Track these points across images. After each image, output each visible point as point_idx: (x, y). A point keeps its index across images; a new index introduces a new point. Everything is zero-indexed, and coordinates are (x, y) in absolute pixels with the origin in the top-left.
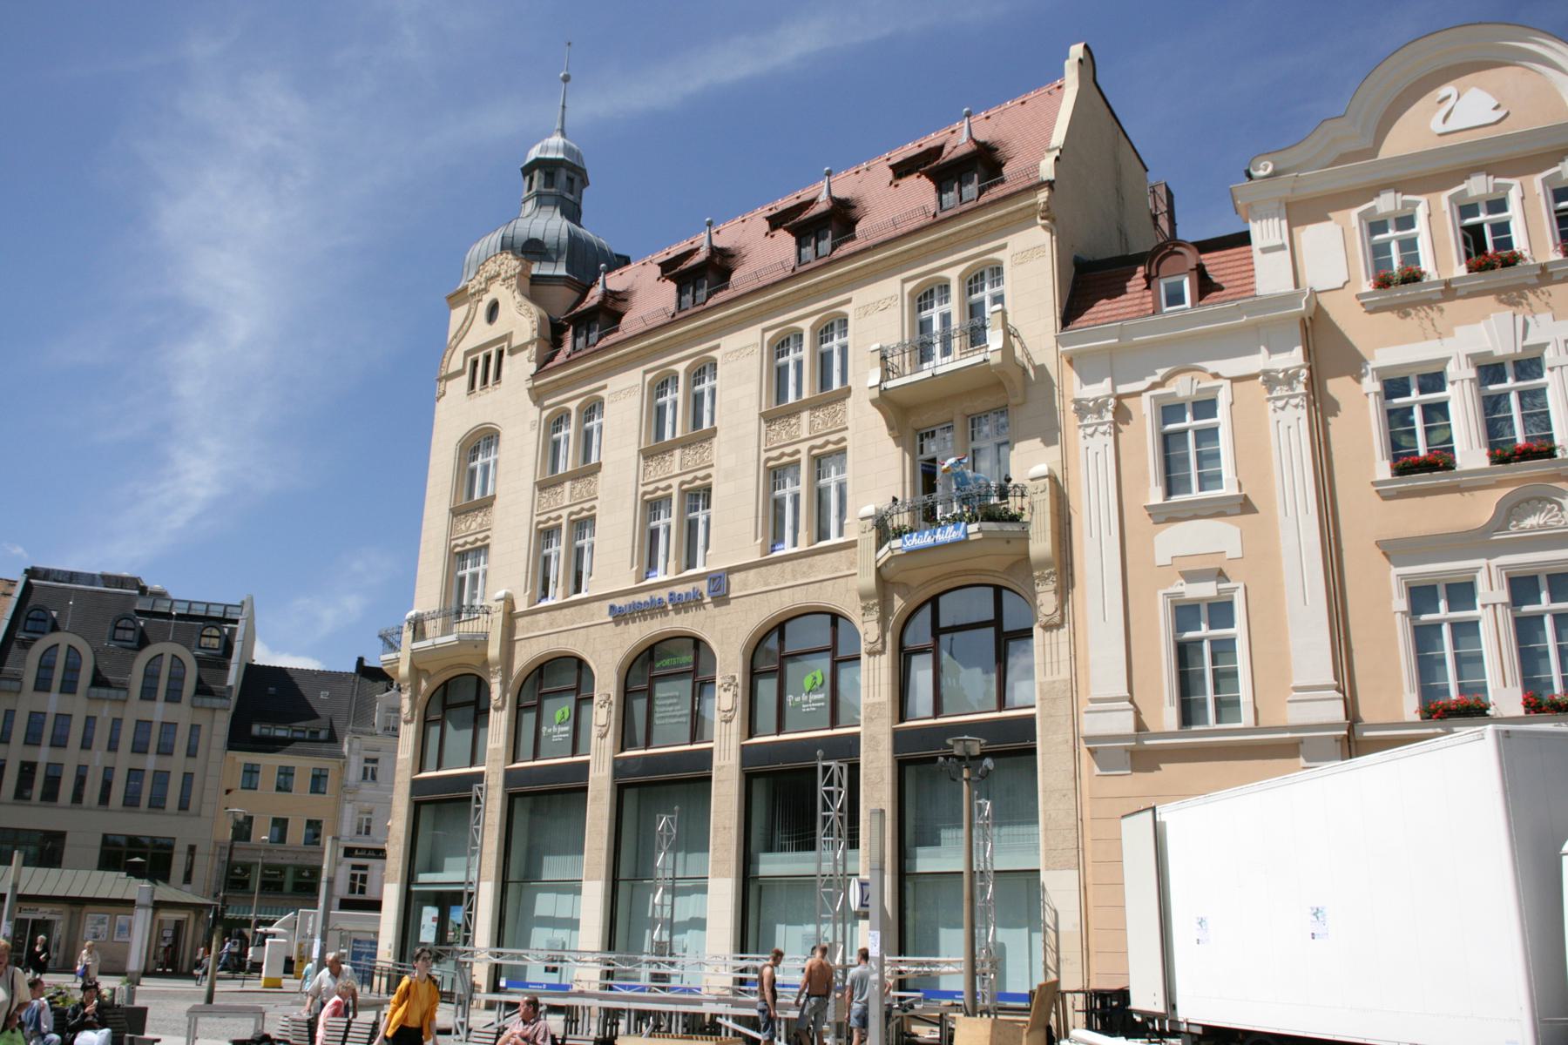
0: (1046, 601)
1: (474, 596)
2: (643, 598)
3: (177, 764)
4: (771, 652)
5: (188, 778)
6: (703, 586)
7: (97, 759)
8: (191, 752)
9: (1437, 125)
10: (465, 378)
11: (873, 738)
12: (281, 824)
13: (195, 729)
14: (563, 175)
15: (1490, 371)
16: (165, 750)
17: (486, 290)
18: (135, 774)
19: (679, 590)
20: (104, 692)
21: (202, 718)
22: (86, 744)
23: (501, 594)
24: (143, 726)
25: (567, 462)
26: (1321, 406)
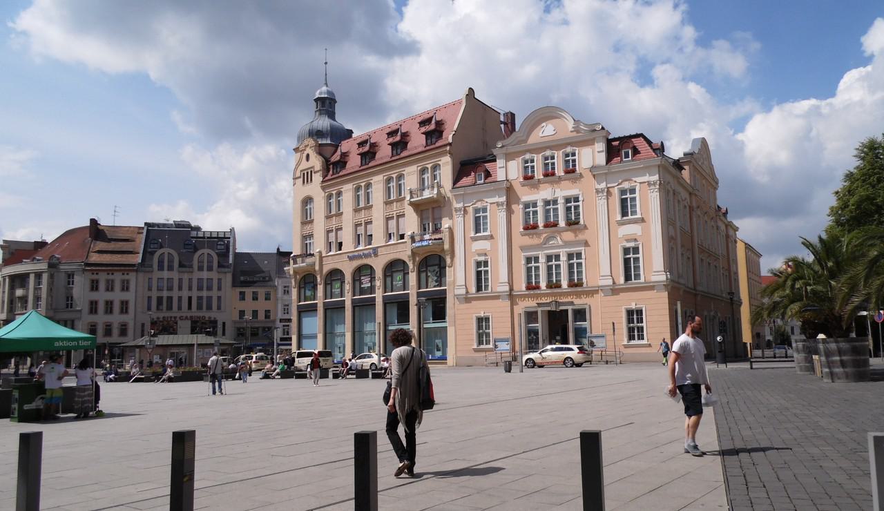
0: (448, 261)
1: (310, 249)
2: (356, 254)
3: (214, 293)
5: (219, 298)
6: (371, 251)
7: (185, 294)
8: (219, 289)
9: (541, 135)
10: (301, 179)
11: (412, 294)
12: (255, 313)
13: (220, 280)
14: (328, 102)
15: (547, 203)
16: (210, 288)
17: (305, 150)
18: (200, 298)
19: (365, 252)
20: (184, 269)
21: (221, 276)
22: (180, 288)
23: (318, 251)
24: (200, 280)
25: (333, 213)
26: (510, 212)
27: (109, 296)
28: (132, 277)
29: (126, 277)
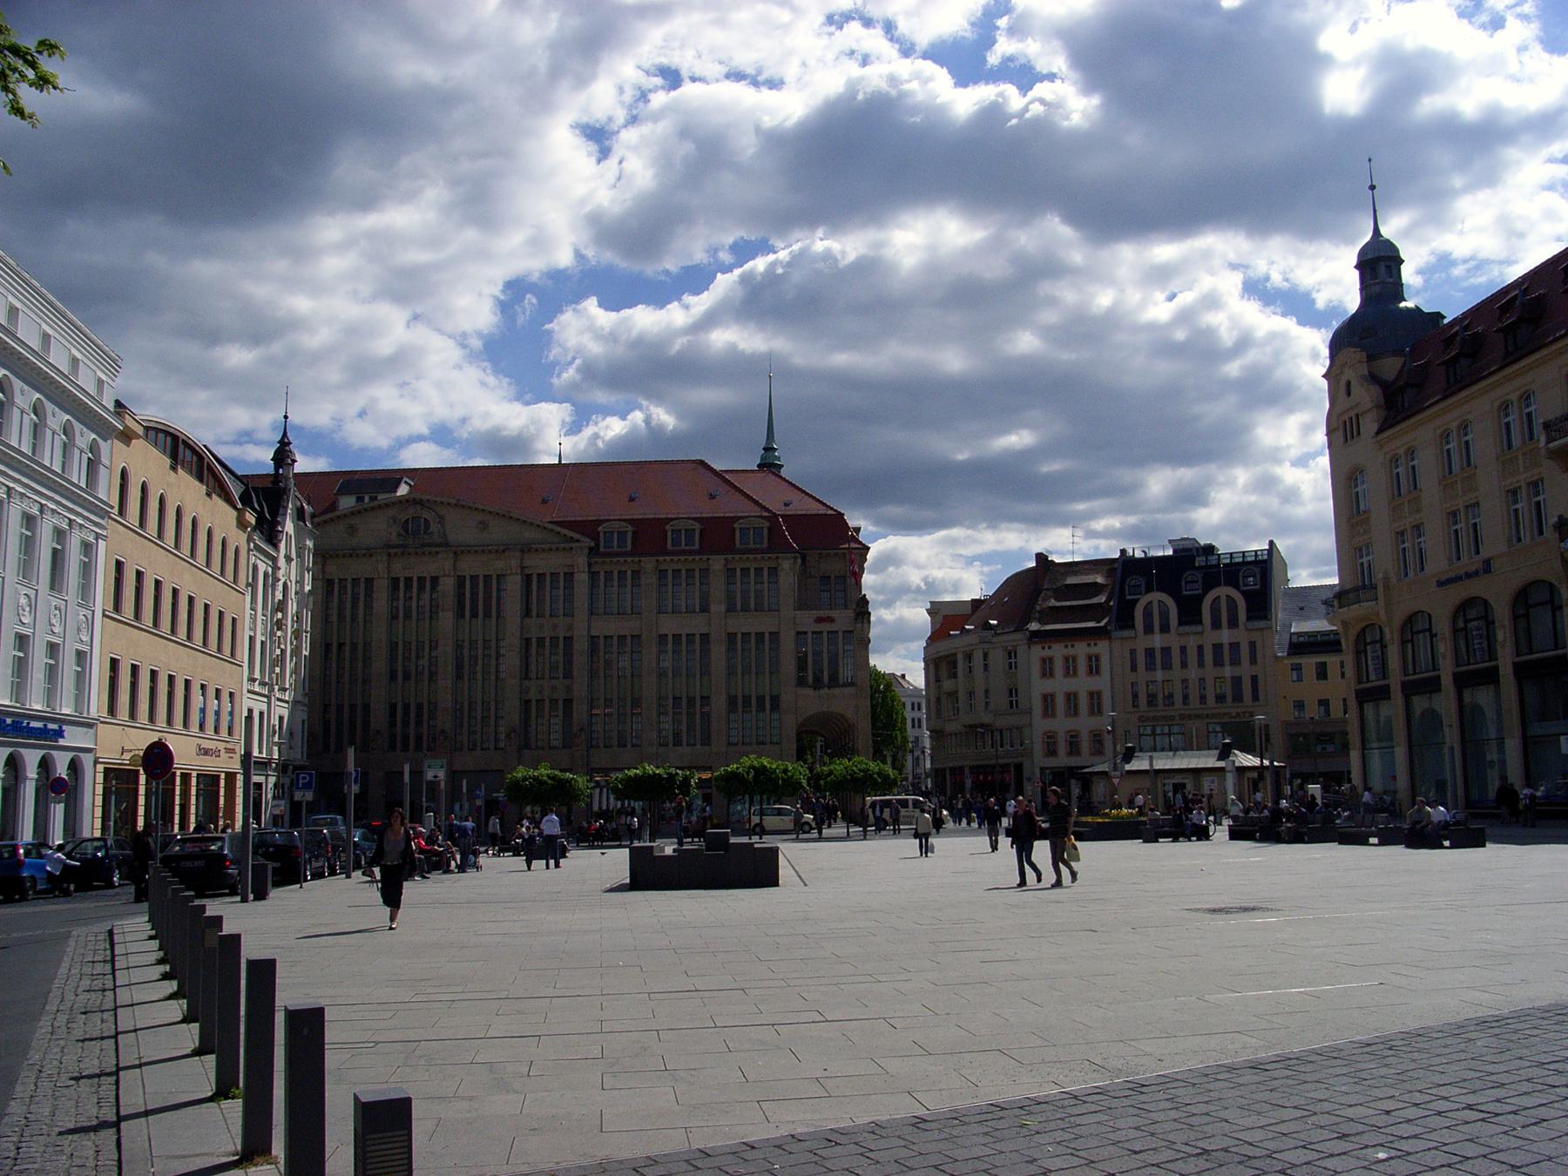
4: (1524, 599)
5: (1254, 679)
7: (1193, 673)
8: (1253, 660)
10: (1341, 432)
12: (1324, 703)
16: (1235, 662)
21: (1255, 636)
22: (1184, 665)
27: (1071, 684)
28: (1102, 647)
29: (1094, 650)
